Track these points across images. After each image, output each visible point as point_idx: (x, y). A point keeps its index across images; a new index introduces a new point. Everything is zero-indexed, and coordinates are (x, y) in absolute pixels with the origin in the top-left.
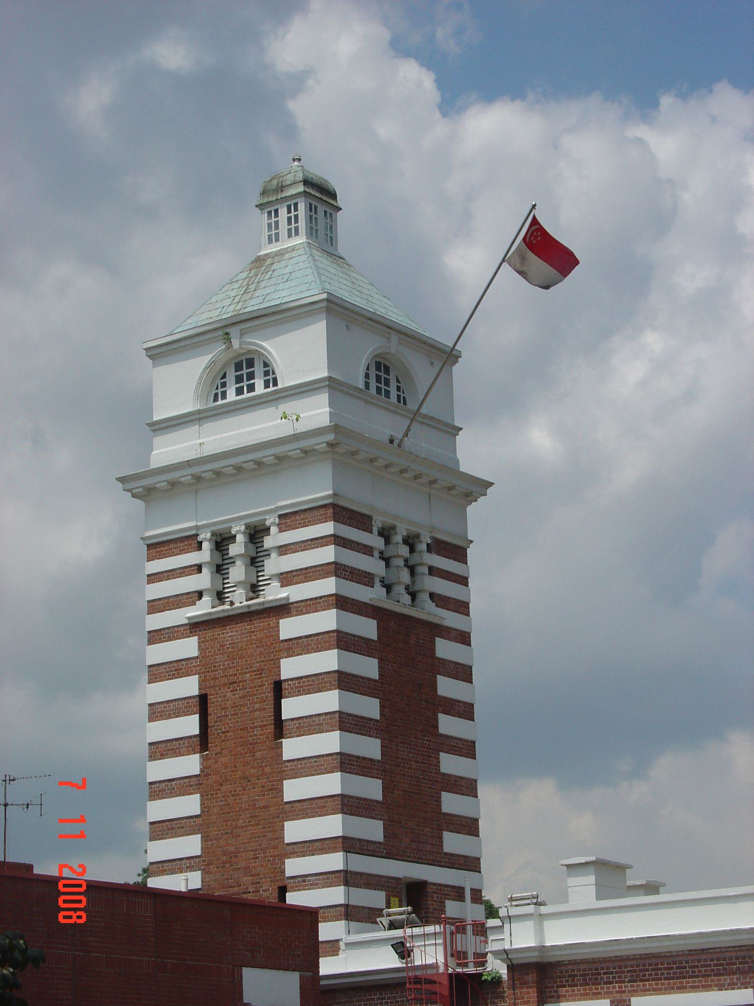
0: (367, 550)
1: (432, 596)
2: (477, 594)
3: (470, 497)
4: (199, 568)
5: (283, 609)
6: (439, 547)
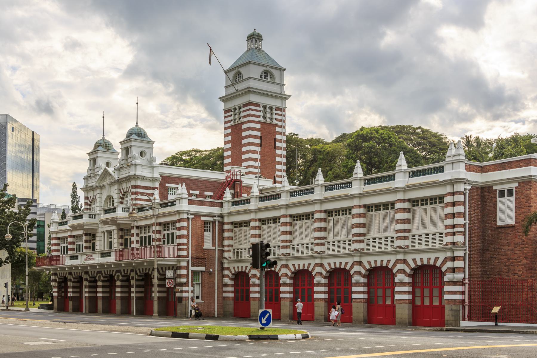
0: (260, 111)
1: (275, 119)
2: (287, 119)
3: (285, 99)
4: (231, 115)
5: (244, 123)
6: (278, 109)
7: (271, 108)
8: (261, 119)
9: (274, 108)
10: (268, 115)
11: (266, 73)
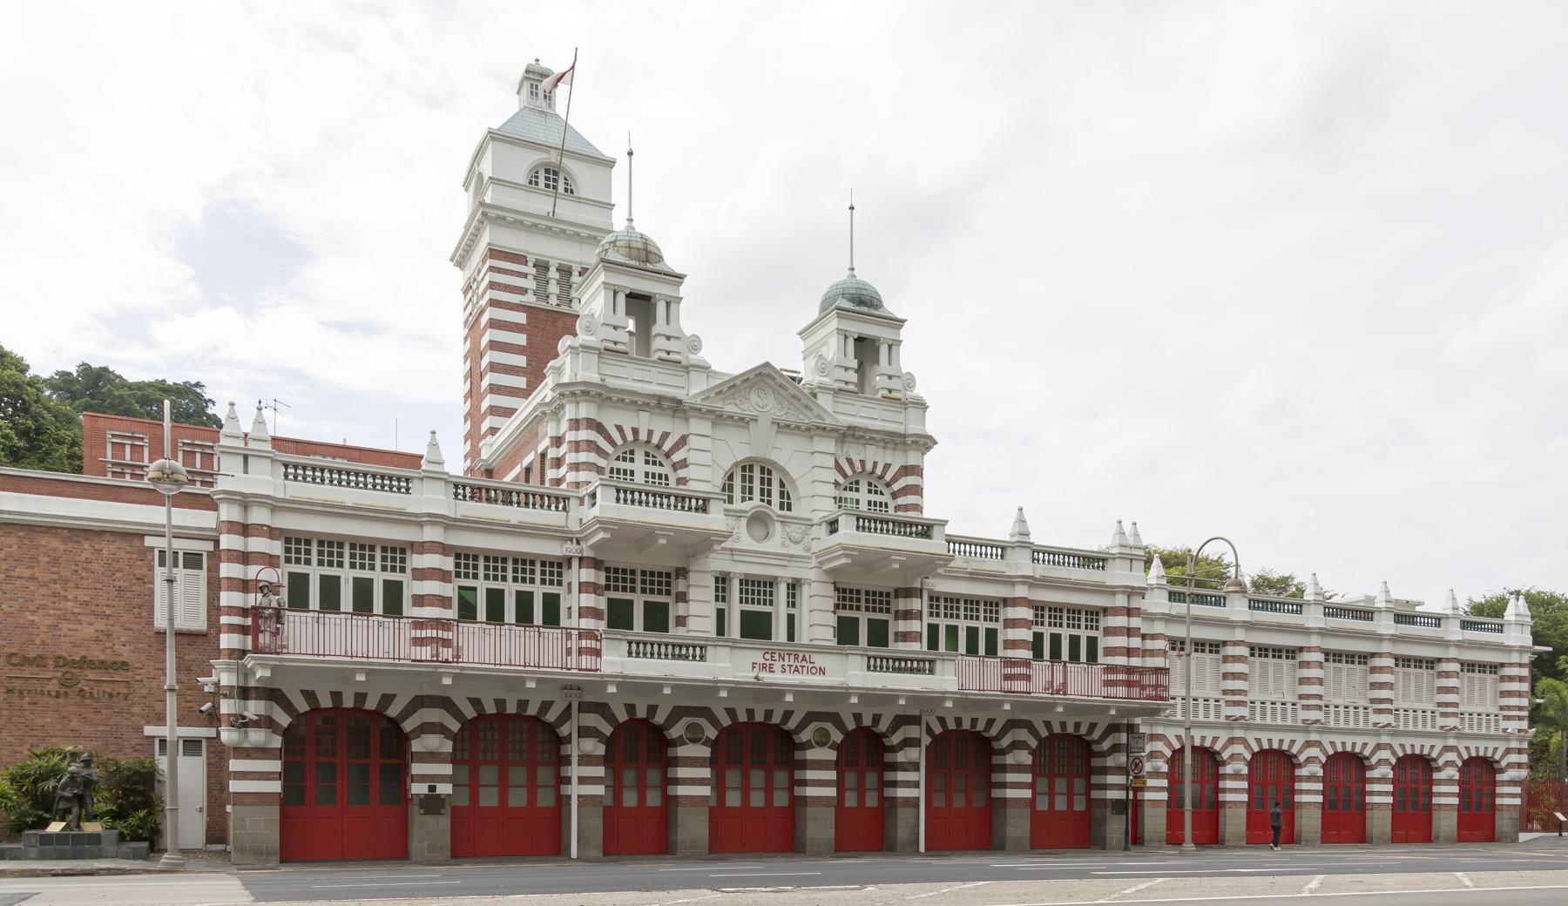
0: (525, 276)
7: (565, 271)
8: (530, 299)
9: (576, 269)
10: (553, 288)
11: (551, 177)
